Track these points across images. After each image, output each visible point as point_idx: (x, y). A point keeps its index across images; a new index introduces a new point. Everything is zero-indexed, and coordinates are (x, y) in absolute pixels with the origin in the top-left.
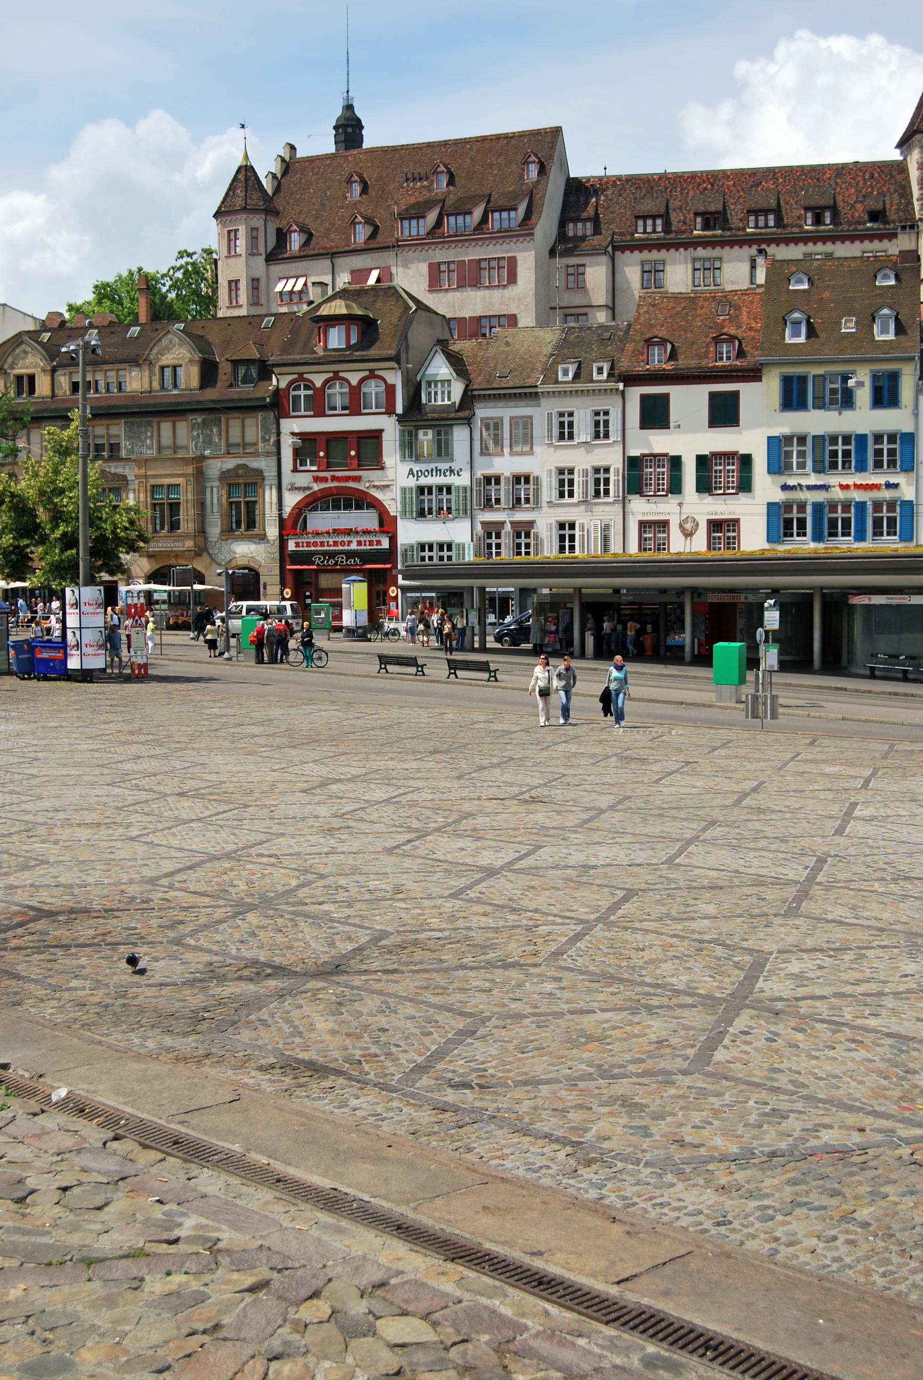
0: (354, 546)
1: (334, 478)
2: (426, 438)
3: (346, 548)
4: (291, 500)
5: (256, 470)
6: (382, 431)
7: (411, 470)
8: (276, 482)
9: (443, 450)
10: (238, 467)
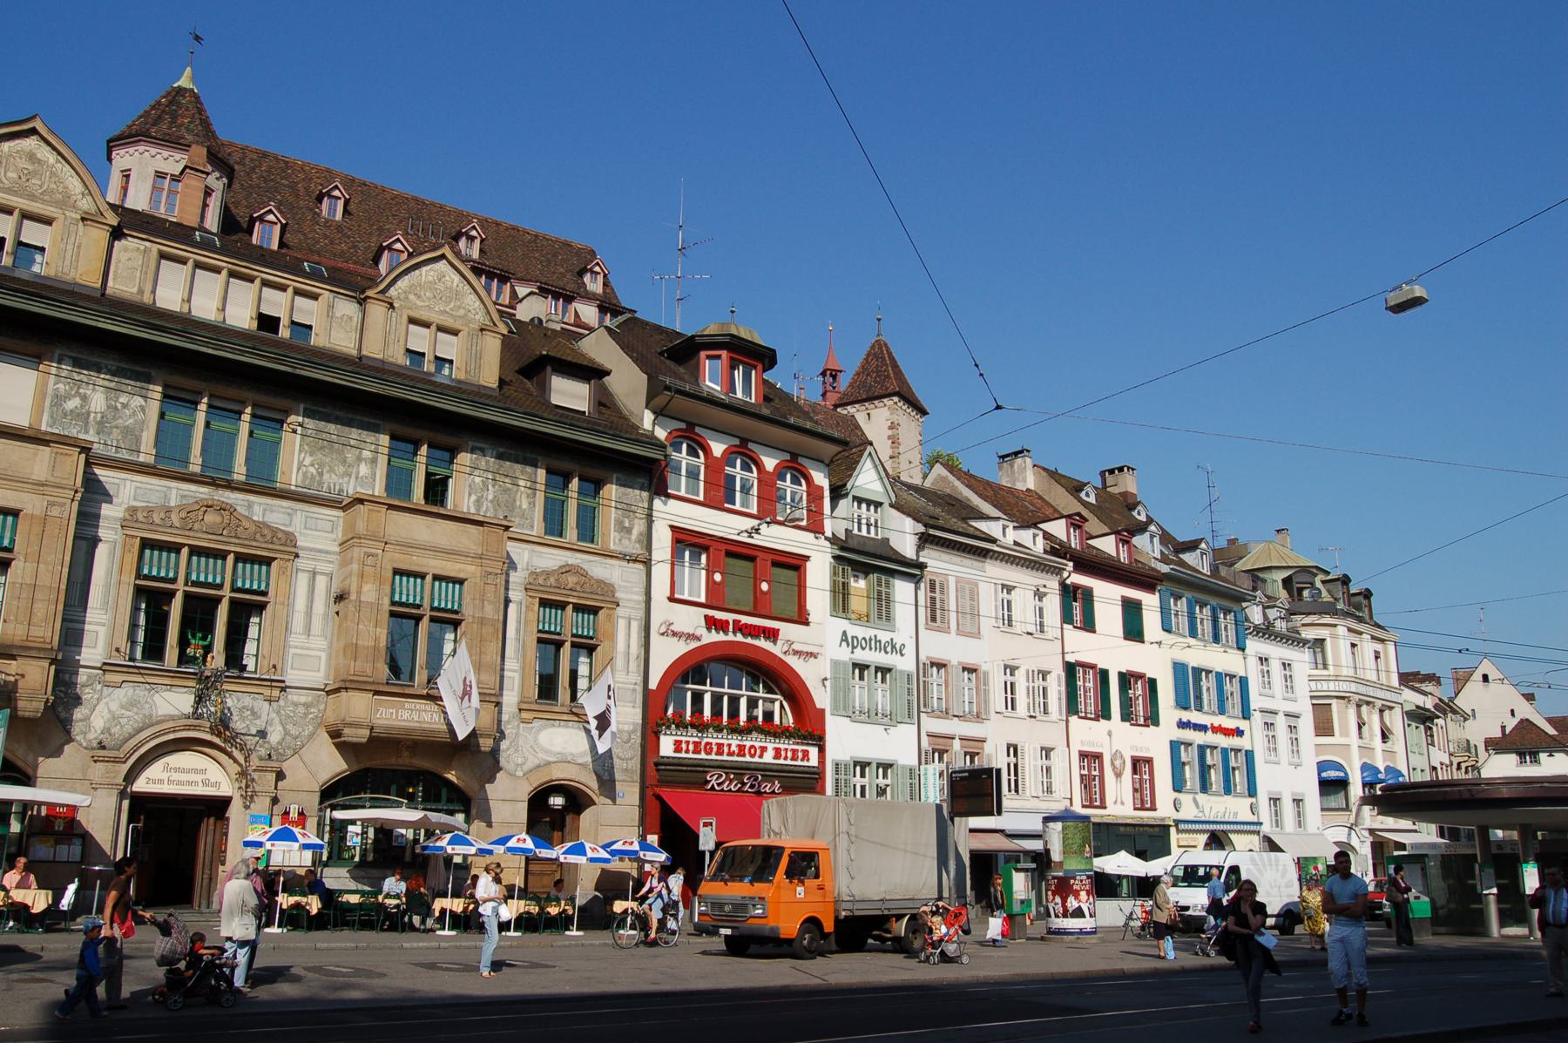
0: (768, 758)
1: (739, 628)
2: (859, 585)
3: (756, 759)
4: (666, 654)
5: (599, 582)
6: (807, 558)
7: (844, 633)
8: (641, 614)
9: (883, 608)
10: (568, 570)
